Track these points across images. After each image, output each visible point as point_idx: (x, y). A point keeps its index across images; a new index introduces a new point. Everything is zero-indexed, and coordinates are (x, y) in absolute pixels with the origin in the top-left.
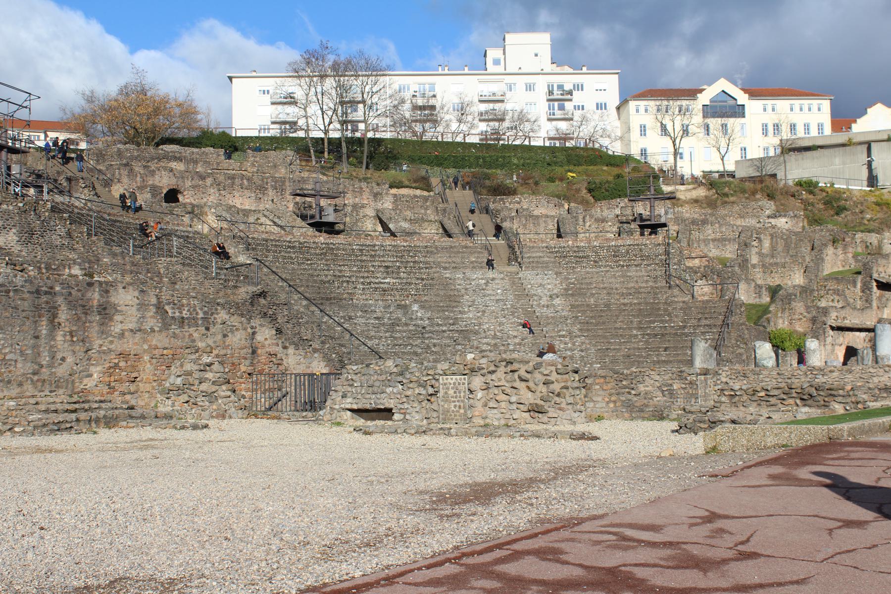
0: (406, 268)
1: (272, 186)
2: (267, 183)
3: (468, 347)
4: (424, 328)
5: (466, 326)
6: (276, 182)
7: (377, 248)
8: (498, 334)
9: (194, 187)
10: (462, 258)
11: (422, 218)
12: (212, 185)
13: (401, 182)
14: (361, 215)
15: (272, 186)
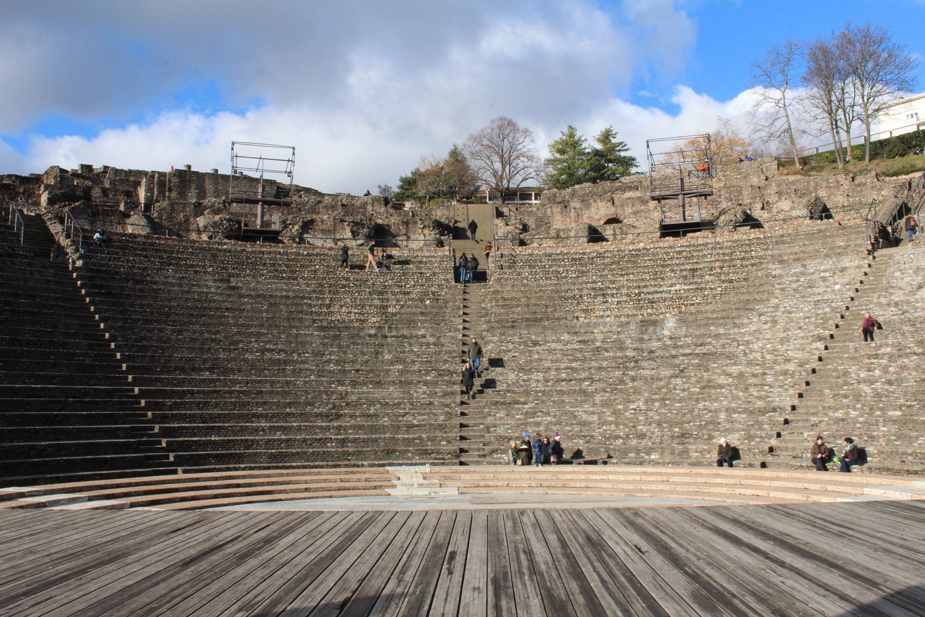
0: (721, 268)
1: (726, 198)
2: (720, 196)
3: (693, 380)
4: (652, 352)
5: (723, 346)
6: (730, 193)
7: (709, 246)
8: (768, 357)
9: (635, 213)
10: (824, 244)
11: (860, 202)
12: (655, 208)
13: (912, 166)
14: (775, 211)
15: (726, 198)
